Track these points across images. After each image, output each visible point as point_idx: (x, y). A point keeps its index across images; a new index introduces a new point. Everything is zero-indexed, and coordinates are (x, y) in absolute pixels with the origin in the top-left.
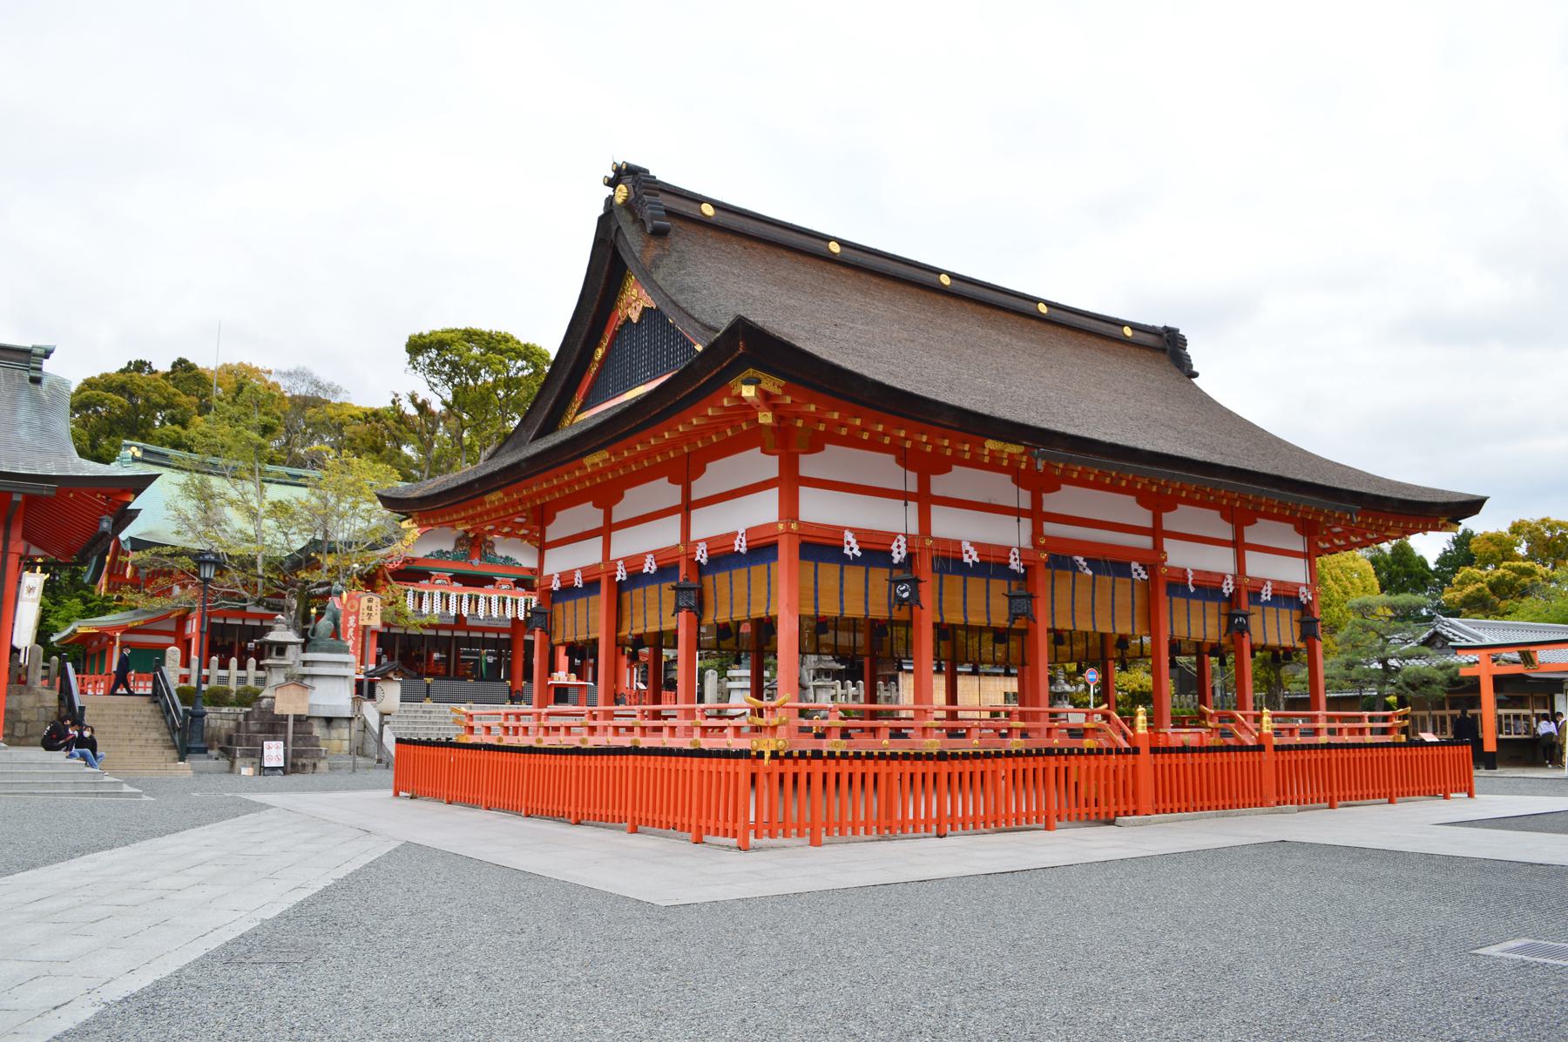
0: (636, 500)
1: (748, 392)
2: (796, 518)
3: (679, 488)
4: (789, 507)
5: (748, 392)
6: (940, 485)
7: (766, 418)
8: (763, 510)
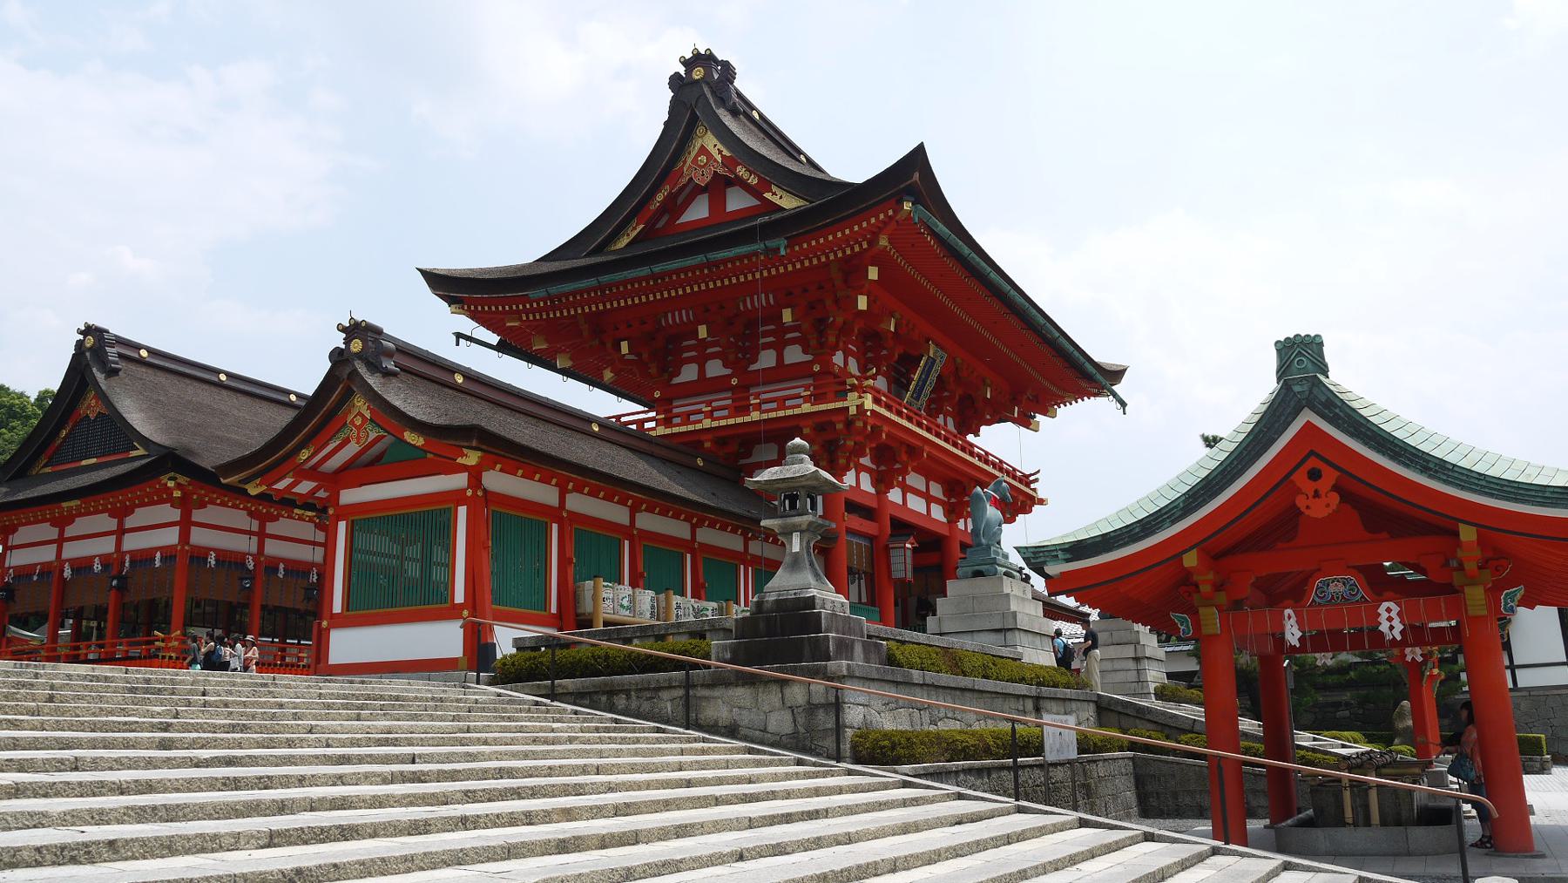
0: (81, 526)
1: (171, 484)
2: (188, 543)
3: (116, 521)
4: (185, 536)
5: (171, 484)
6: (271, 528)
7: (177, 494)
8: (171, 537)
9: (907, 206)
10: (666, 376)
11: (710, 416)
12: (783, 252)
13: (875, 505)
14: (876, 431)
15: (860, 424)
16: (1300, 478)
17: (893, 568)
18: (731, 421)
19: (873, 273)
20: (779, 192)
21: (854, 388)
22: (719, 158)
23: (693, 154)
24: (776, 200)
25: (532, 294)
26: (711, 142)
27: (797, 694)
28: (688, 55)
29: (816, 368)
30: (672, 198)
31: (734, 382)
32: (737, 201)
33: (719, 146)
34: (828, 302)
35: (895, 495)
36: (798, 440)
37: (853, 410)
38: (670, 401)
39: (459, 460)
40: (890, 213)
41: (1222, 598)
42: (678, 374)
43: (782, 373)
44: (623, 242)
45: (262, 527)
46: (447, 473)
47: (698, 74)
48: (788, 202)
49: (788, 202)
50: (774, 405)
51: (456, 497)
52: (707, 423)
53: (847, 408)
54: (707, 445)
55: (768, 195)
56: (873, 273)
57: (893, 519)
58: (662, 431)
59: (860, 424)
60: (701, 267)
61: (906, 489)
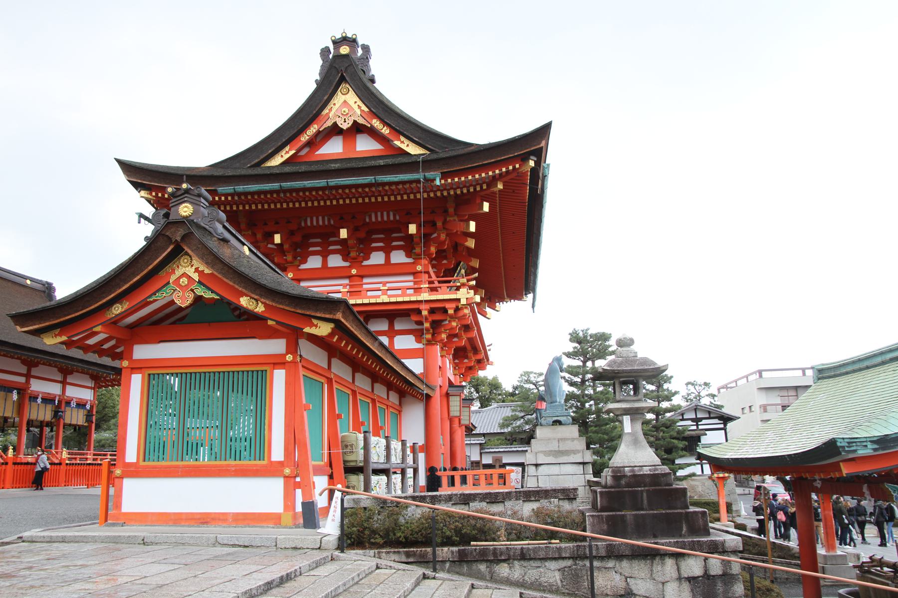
10: (297, 263)
12: (438, 183)
17: (451, 409)
19: (486, 207)
20: (407, 142)
22: (359, 112)
23: (337, 106)
24: (403, 147)
25: (221, 189)
26: (352, 98)
27: (693, 566)
28: (338, 36)
30: (318, 133)
32: (365, 145)
33: (360, 103)
34: (439, 224)
37: (463, 302)
39: (307, 330)
40: (517, 166)
42: (305, 262)
43: (388, 270)
44: (277, 161)
45: (29, 371)
46: (261, 337)
47: (344, 50)
48: (413, 150)
49: (413, 150)
50: (399, 292)
51: (277, 362)
53: (459, 300)
55: (397, 143)
60: (369, 185)
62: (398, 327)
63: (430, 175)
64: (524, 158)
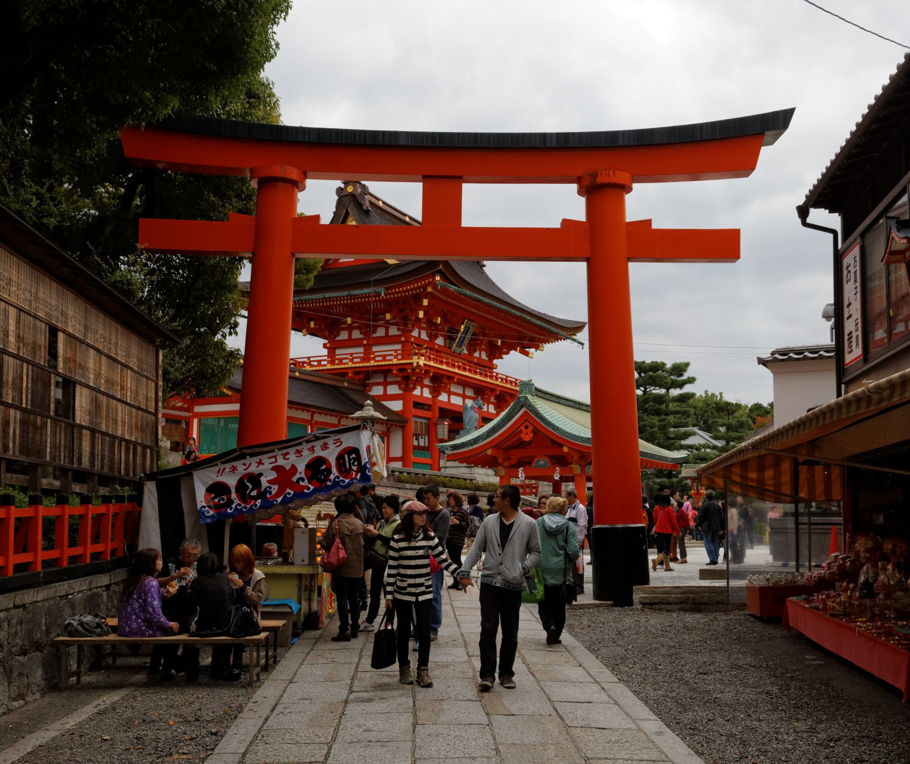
9: (438, 278)
11: (351, 358)
13: (430, 403)
14: (426, 371)
15: (418, 370)
16: (522, 428)
18: (361, 365)
19: (425, 302)
21: (416, 354)
29: (403, 339)
31: (365, 342)
35: (443, 397)
36: (369, 402)
37: (415, 365)
38: (335, 349)
41: (506, 464)
42: (338, 335)
43: (387, 340)
50: (380, 358)
52: (350, 365)
54: (350, 375)
56: (425, 302)
57: (440, 409)
58: (329, 367)
59: (418, 370)
61: (450, 393)
62: (389, 380)
63: (378, 290)
64: (434, 275)
